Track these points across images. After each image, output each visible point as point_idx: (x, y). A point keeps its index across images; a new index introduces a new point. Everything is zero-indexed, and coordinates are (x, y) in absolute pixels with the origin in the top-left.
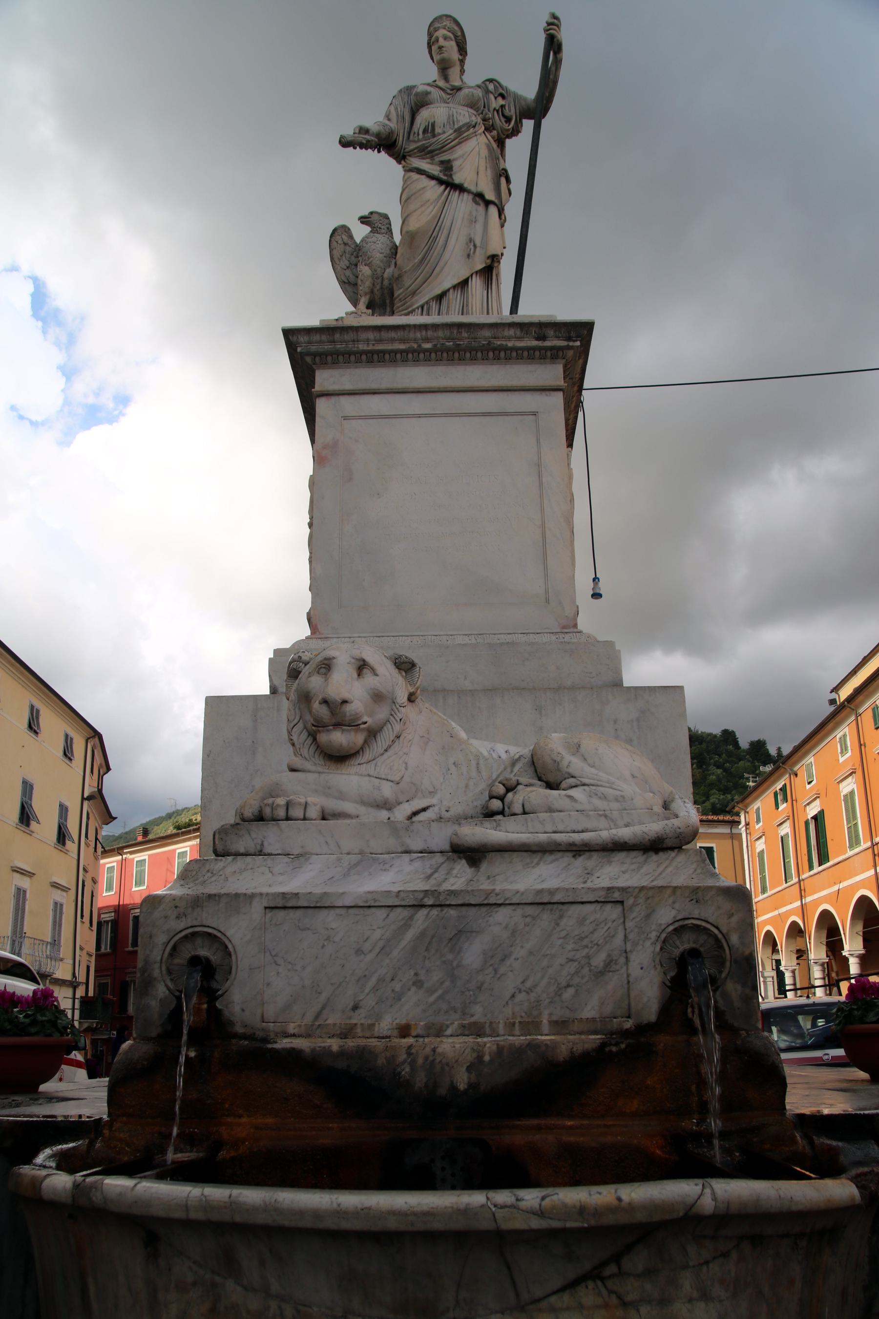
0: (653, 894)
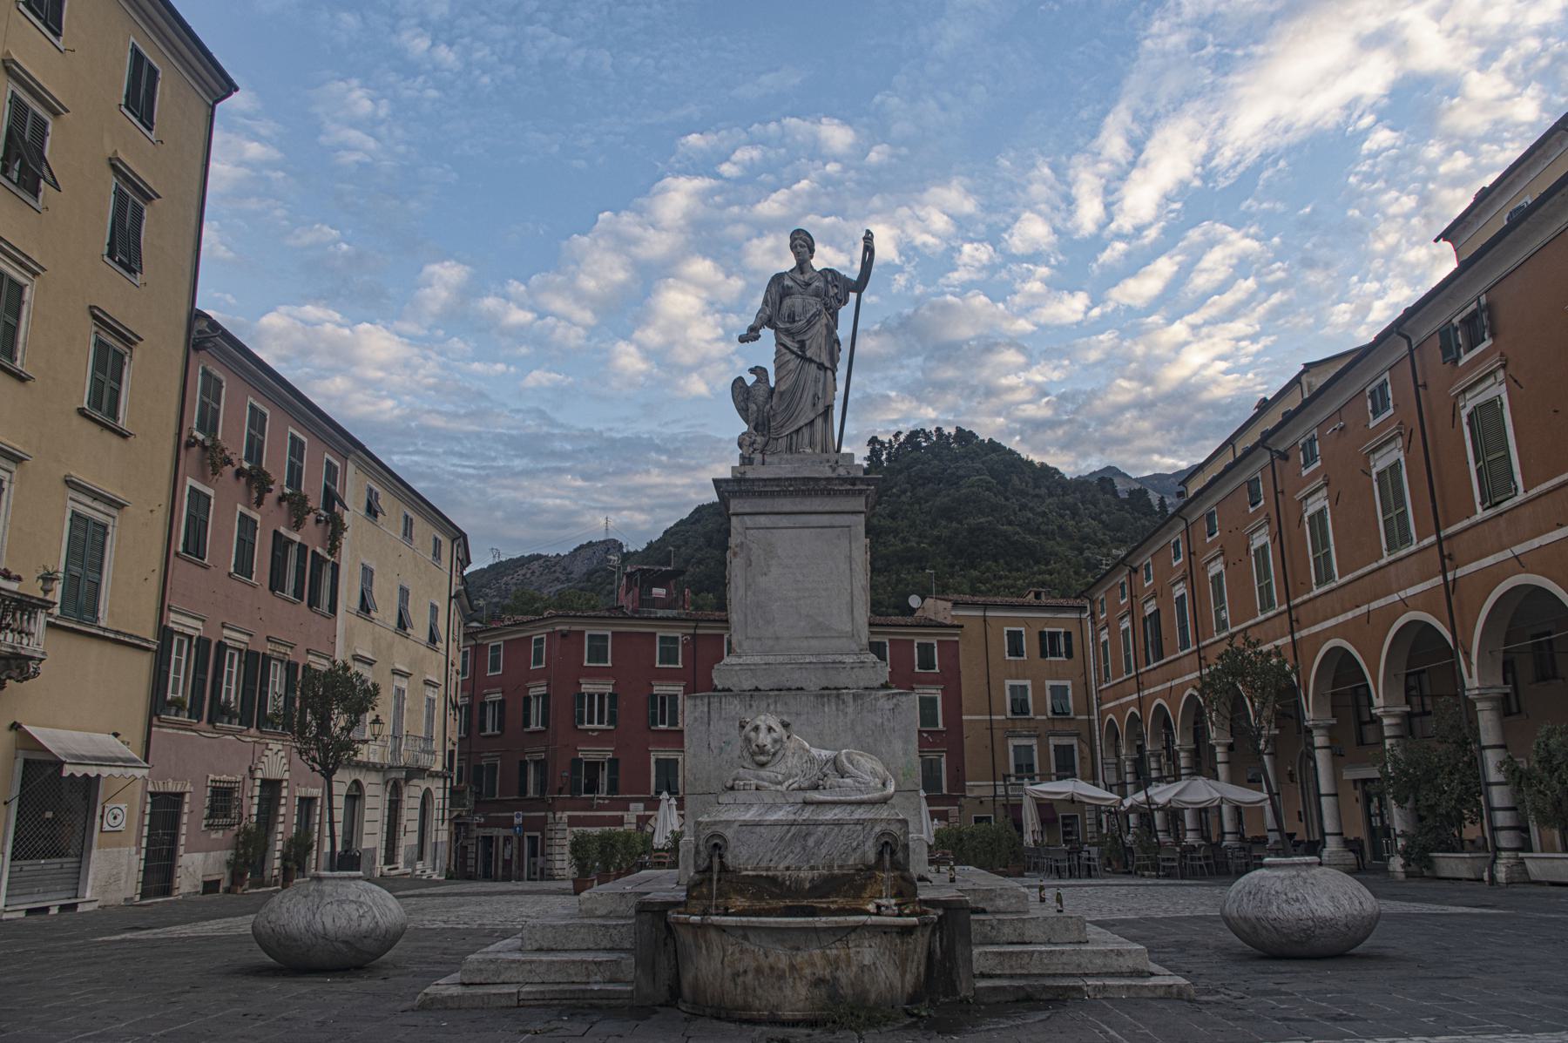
0: (874, 821)
